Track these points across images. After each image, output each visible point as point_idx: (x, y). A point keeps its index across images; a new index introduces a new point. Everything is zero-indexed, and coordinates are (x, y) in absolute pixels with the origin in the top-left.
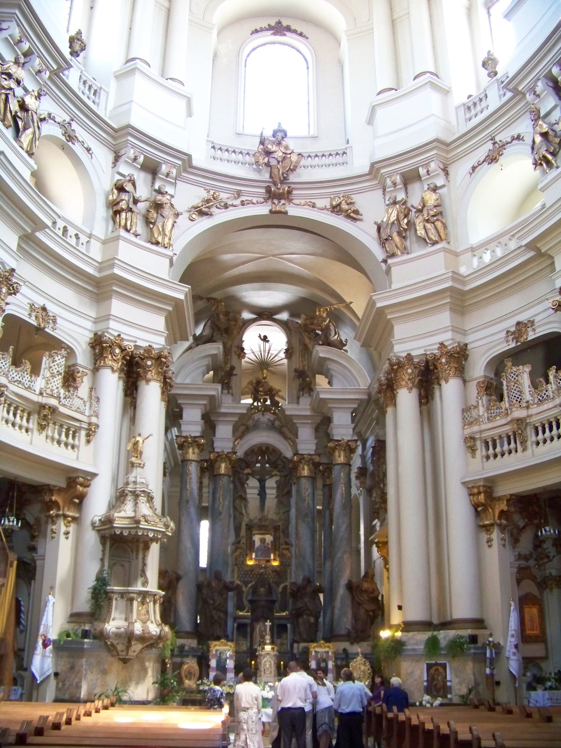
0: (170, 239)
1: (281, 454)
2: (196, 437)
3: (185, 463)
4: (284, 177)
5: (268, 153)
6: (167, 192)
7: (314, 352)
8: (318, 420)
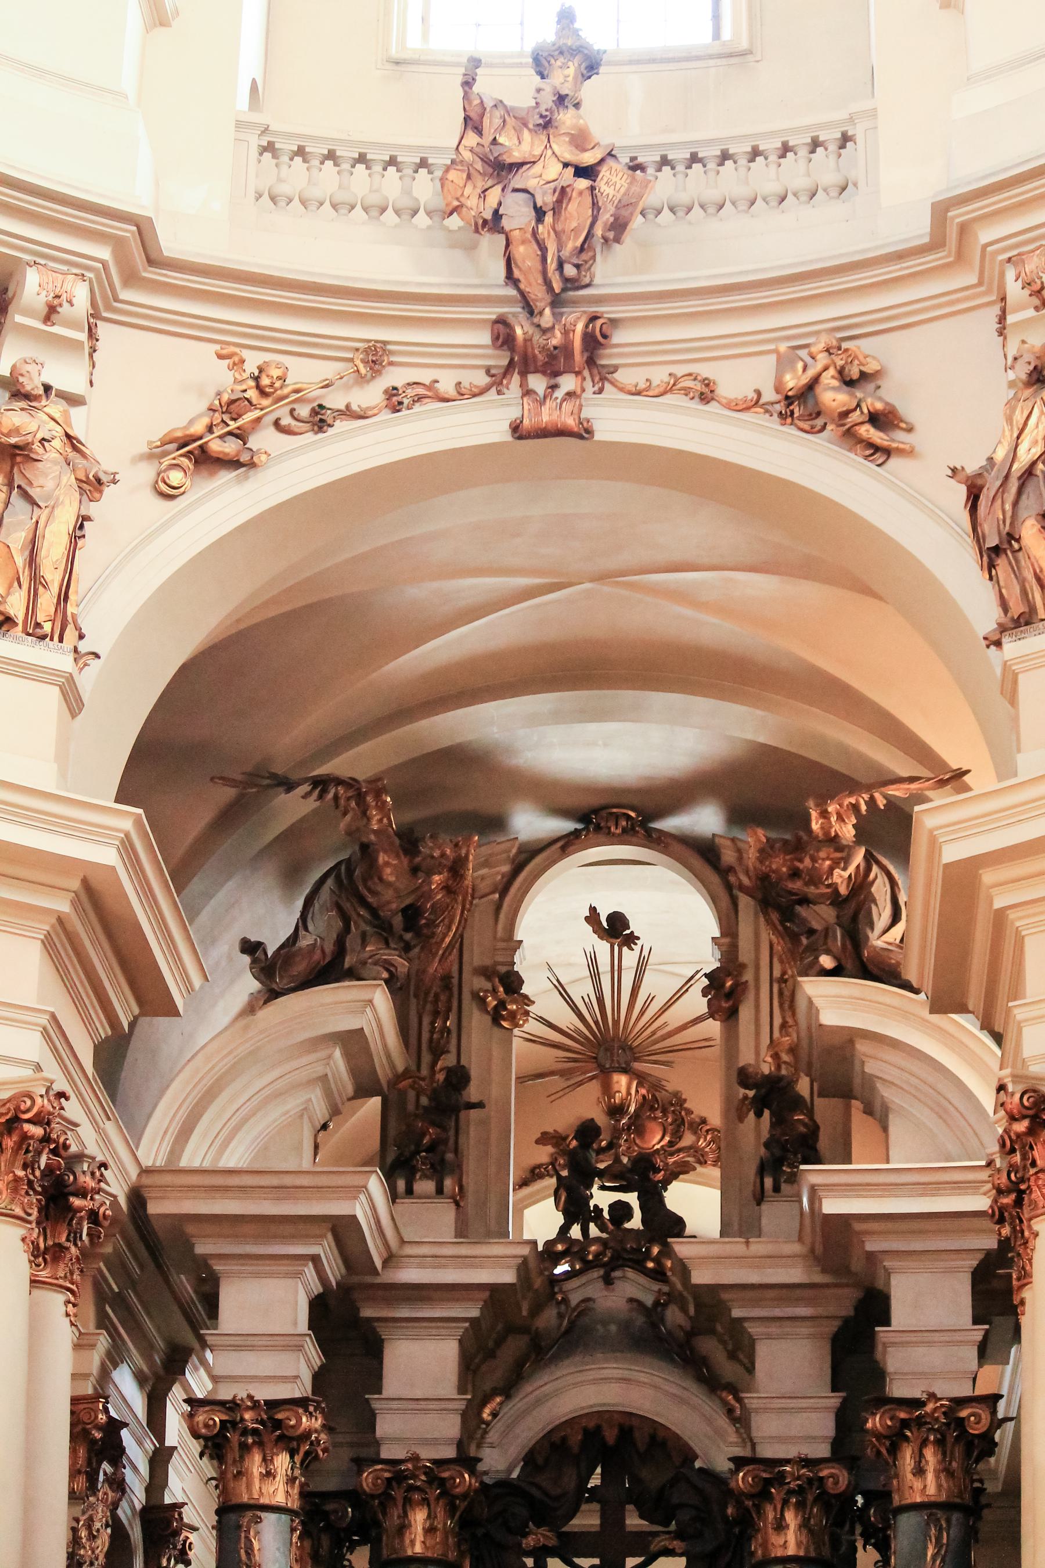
0: (64, 597)
1: (690, 1456)
2: (273, 1405)
3: (233, 1517)
4: (566, 280)
5: (502, 169)
6: (47, 388)
7: (801, 1005)
8: (842, 1304)
